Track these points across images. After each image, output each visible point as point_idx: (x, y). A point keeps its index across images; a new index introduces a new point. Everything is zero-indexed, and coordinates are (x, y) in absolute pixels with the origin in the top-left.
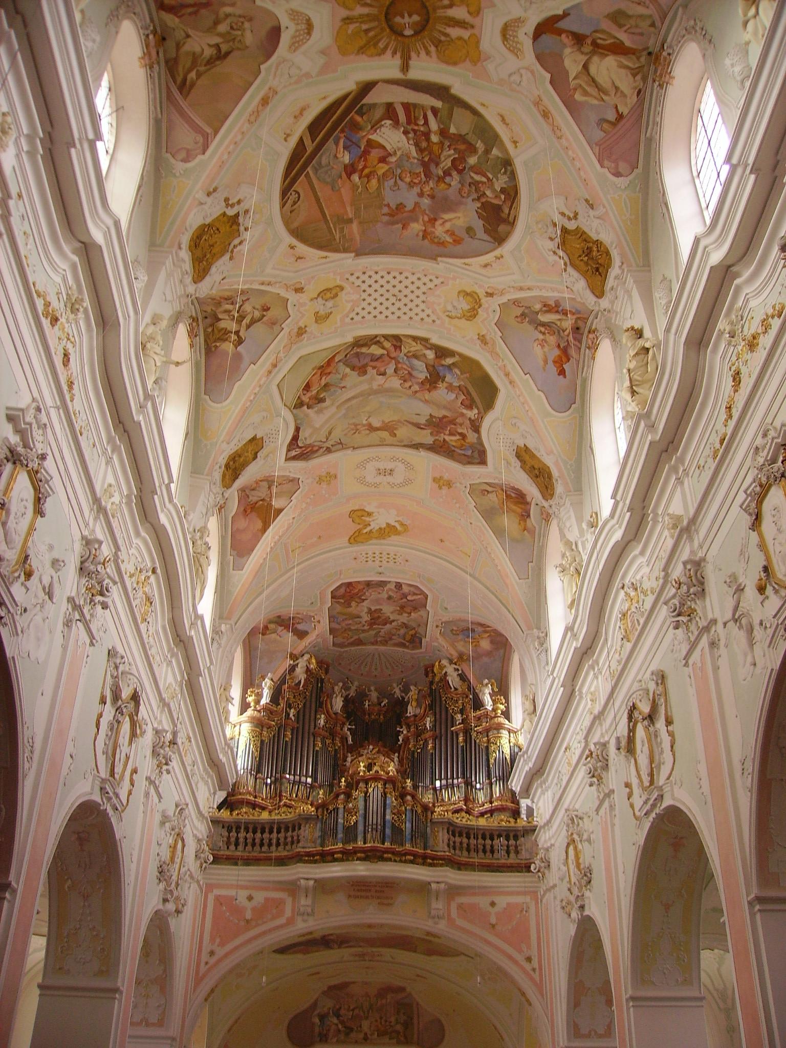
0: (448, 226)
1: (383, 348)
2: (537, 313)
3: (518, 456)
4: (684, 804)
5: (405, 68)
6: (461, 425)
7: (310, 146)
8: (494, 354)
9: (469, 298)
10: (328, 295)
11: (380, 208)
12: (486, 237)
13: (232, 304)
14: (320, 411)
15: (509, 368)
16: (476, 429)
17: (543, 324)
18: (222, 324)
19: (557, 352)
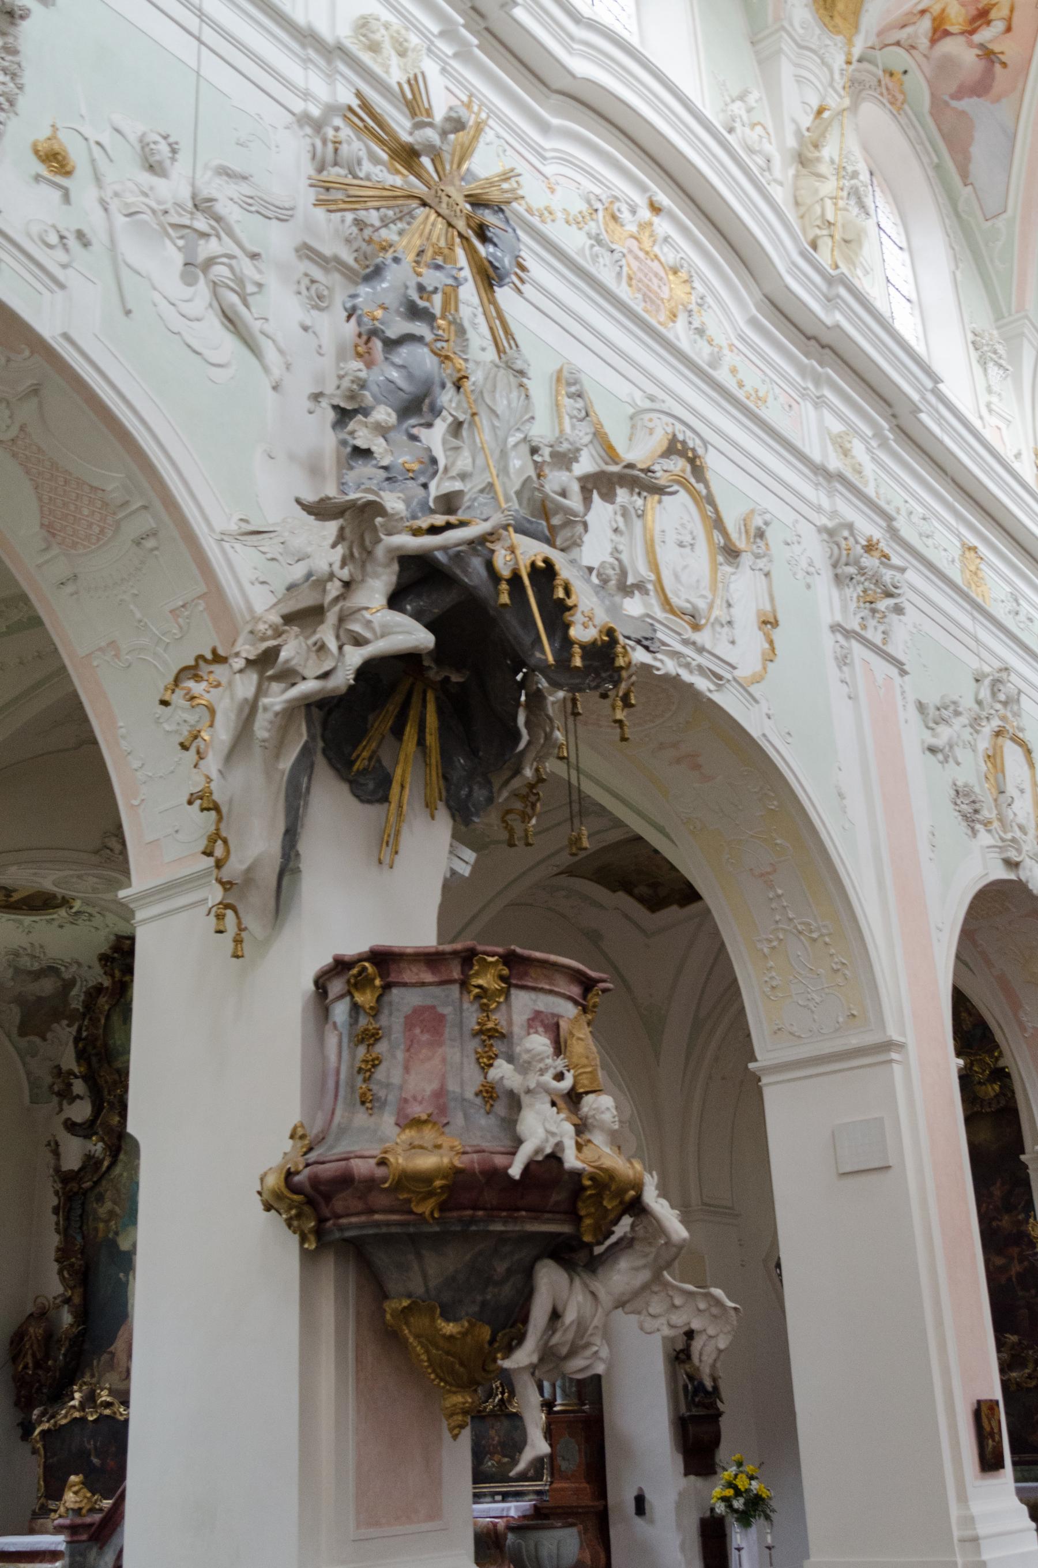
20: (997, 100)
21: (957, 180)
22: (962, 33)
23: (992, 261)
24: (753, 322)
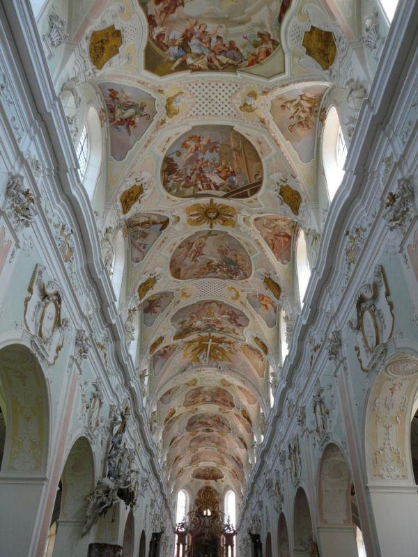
0: (189, 150)
1: (219, 60)
2: (136, 114)
3: (118, 34)
4: (9, 340)
5: (212, 201)
6: (162, 12)
7: (248, 190)
8: (154, 88)
9: (173, 112)
10: (248, 108)
11: (220, 151)
12: (171, 156)
13: (300, 117)
14: (262, 25)
15: (143, 86)
16: (151, 20)
17: (130, 107)
18: (309, 105)
19: (118, 96)
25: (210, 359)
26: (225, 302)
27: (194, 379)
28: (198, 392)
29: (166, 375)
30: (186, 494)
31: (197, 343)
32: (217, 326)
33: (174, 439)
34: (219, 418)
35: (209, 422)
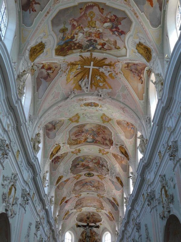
20: (47, 81)
21: (36, 90)
22: (46, 69)
23: (36, 105)
24: (4, 100)
25: (91, 87)
26: (108, 4)
27: (77, 114)
28: (80, 130)
29: (50, 100)
30: (71, 235)
31: (79, 67)
32: (98, 42)
33: (60, 178)
34: (99, 161)
35: (91, 165)
